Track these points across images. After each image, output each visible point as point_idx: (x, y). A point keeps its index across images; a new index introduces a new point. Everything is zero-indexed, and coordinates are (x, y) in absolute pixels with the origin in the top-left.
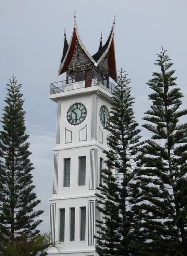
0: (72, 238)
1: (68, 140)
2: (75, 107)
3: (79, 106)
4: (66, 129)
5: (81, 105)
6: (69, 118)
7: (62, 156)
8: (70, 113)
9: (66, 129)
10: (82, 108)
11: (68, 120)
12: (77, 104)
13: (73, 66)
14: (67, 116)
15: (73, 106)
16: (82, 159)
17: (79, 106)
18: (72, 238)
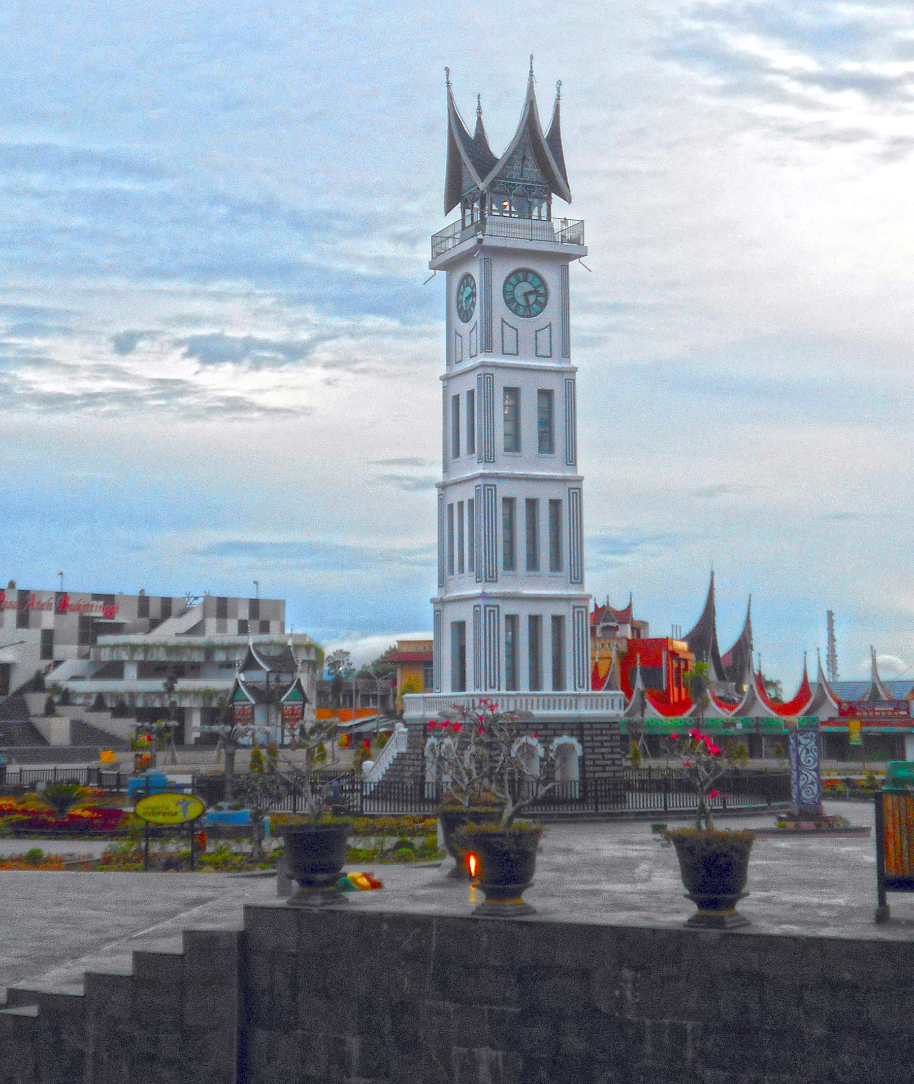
0: (533, 563)
1: (510, 346)
2: (521, 275)
3: (530, 277)
4: (503, 321)
5: (536, 275)
6: (508, 297)
7: (502, 380)
8: (509, 288)
9: (503, 321)
10: (537, 282)
11: (508, 303)
12: (526, 271)
13: (507, 179)
14: (504, 291)
15: (515, 273)
16: (546, 395)
17: (530, 277)
18: (533, 563)
